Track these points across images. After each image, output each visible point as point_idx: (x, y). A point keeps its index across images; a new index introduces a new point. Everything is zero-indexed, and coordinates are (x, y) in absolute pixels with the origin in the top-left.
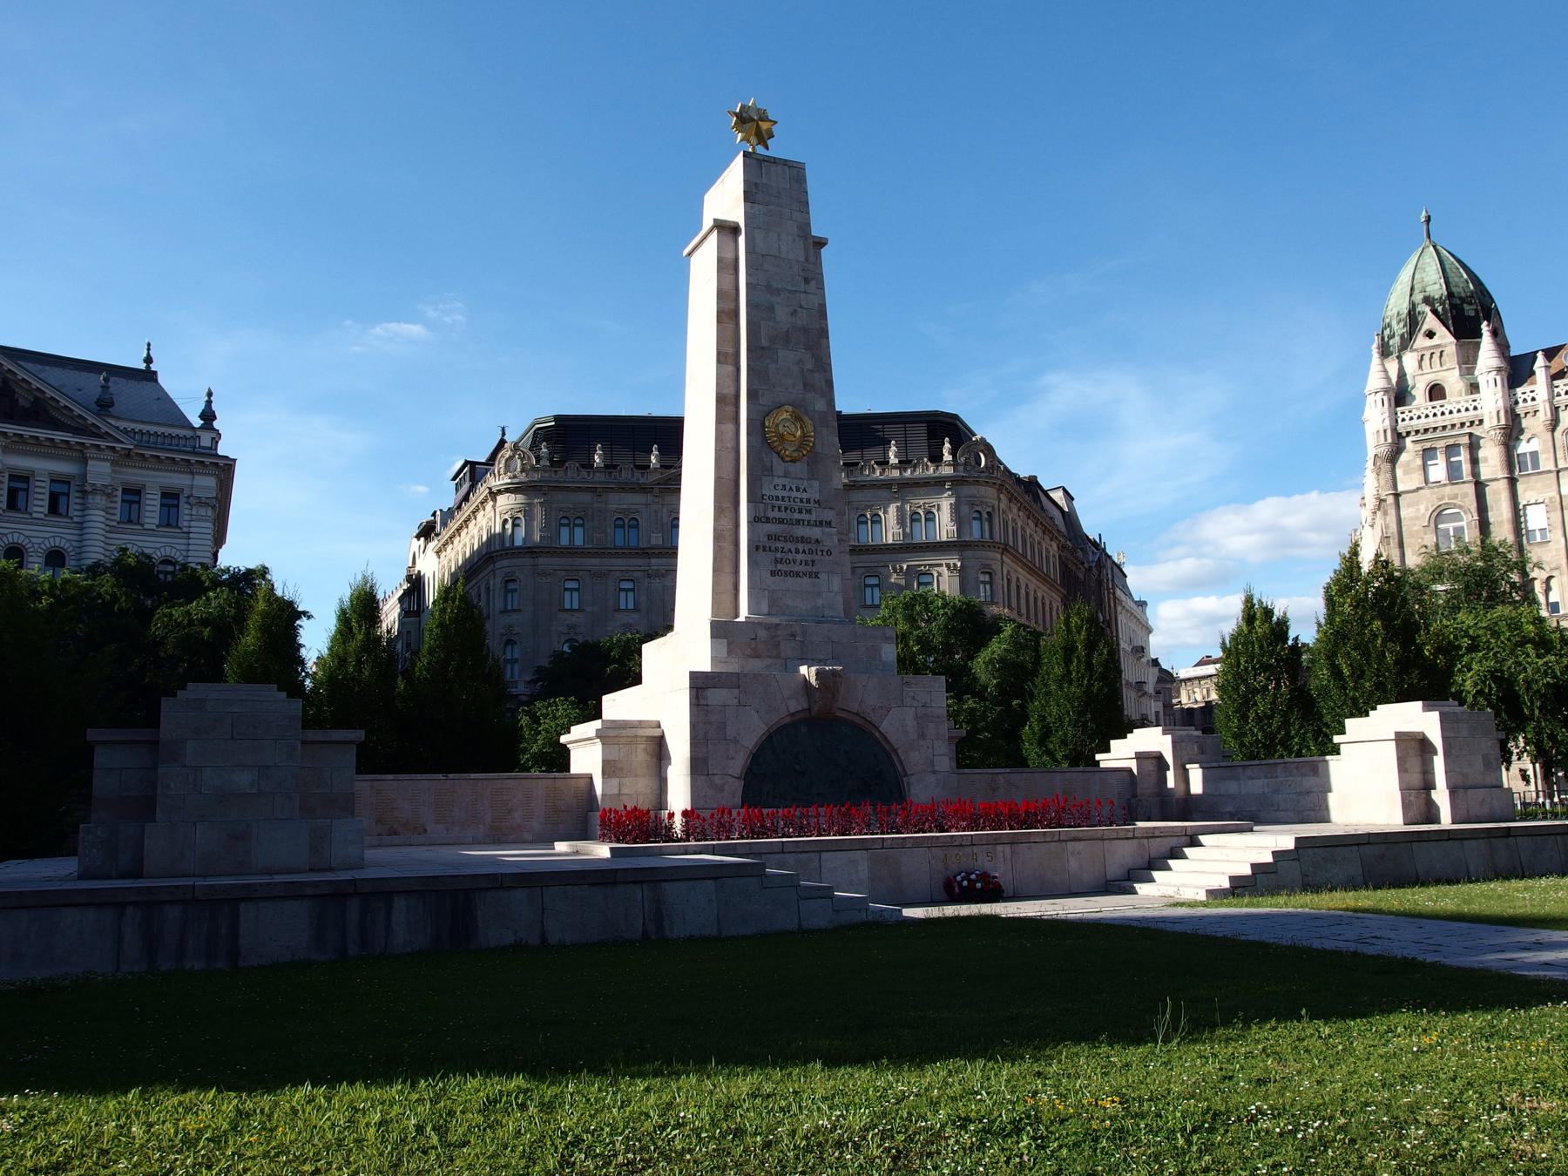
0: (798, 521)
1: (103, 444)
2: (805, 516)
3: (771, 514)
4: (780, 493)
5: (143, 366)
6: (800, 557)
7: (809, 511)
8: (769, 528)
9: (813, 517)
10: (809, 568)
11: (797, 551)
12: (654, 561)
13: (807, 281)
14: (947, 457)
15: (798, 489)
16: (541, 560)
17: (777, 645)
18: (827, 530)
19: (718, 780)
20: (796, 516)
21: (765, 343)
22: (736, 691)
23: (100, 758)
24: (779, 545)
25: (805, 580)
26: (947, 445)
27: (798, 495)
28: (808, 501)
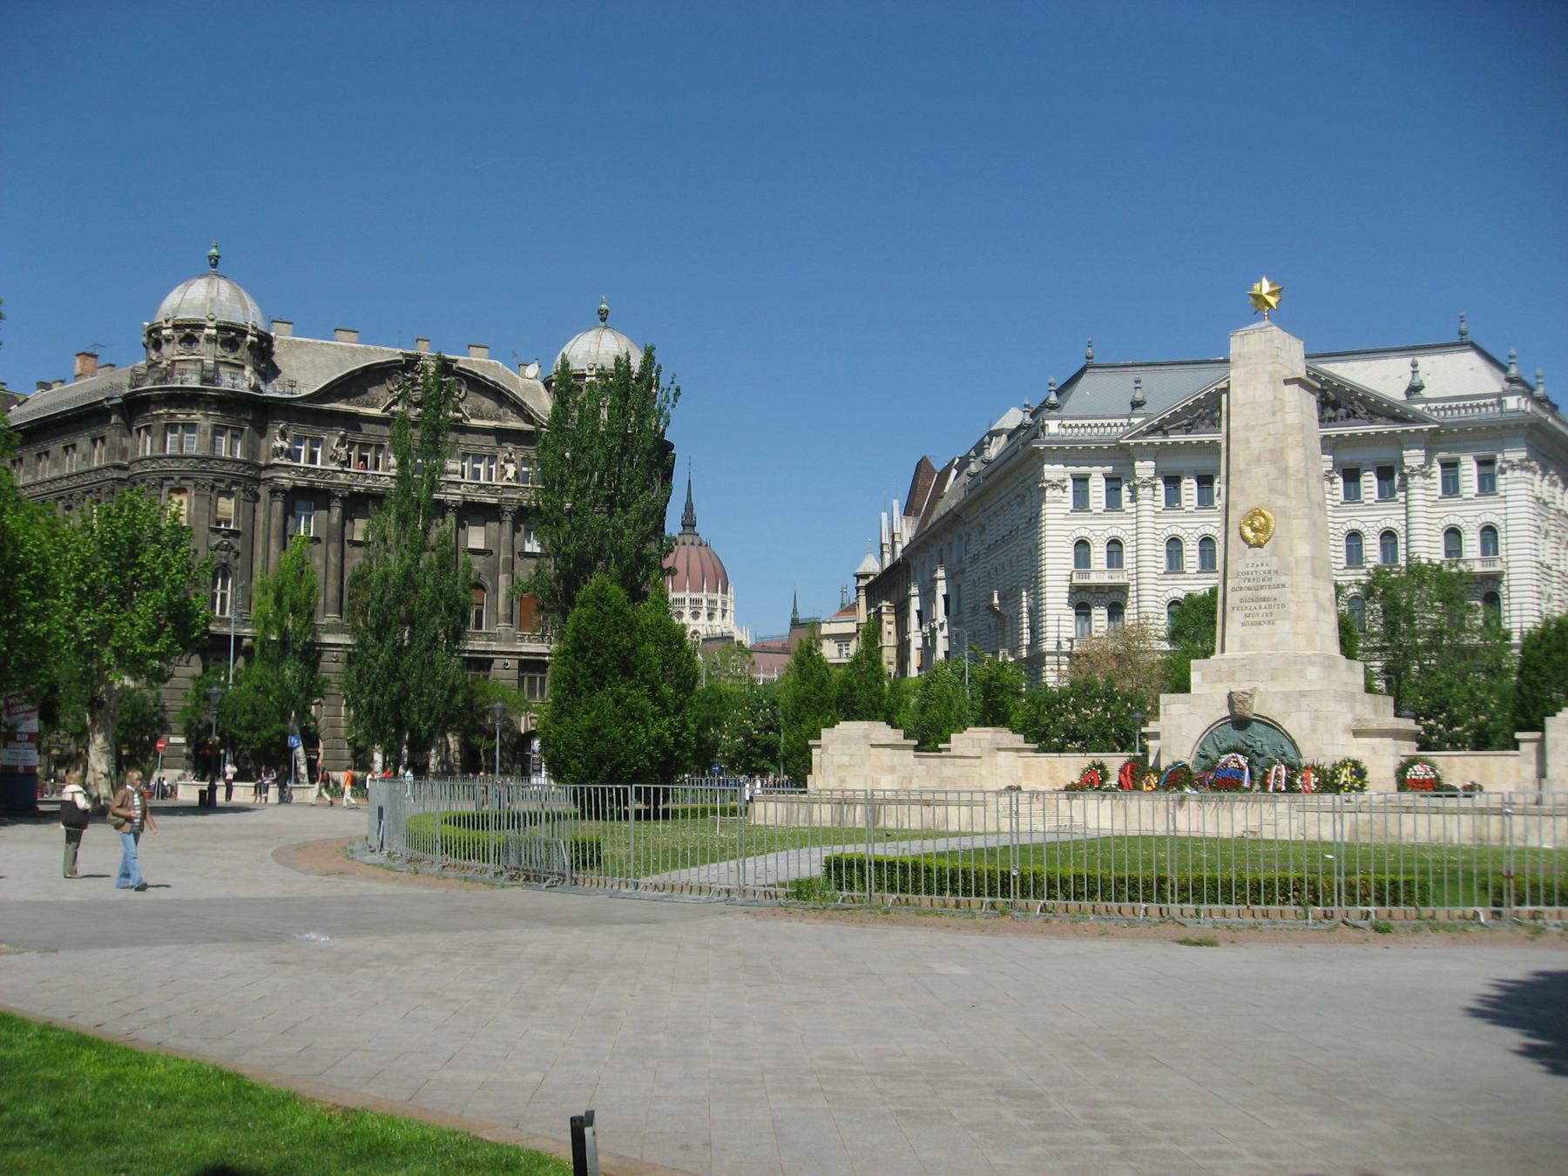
1: (1412, 428)
3: (1243, 585)
4: (1250, 569)
5: (1457, 339)
9: (1273, 582)
17: (1233, 673)
21: (1242, 466)
23: (814, 751)
25: (1265, 627)
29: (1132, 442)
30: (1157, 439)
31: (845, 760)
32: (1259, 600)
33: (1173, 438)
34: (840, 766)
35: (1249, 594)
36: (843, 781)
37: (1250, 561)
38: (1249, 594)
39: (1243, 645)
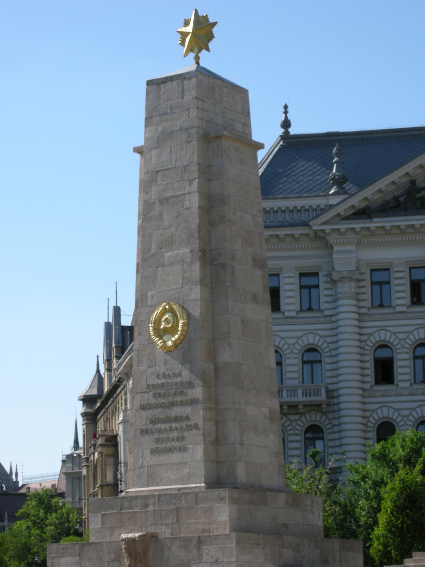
2: (178, 399)
6: (175, 434)
7: (182, 393)
8: (150, 412)
21: (153, 251)
24: (158, 426)
29: (327, 228)
30: (358, 225)
32: (168, 420)
33: (376, 223)
35: (158, 412)
38: (158, 412)
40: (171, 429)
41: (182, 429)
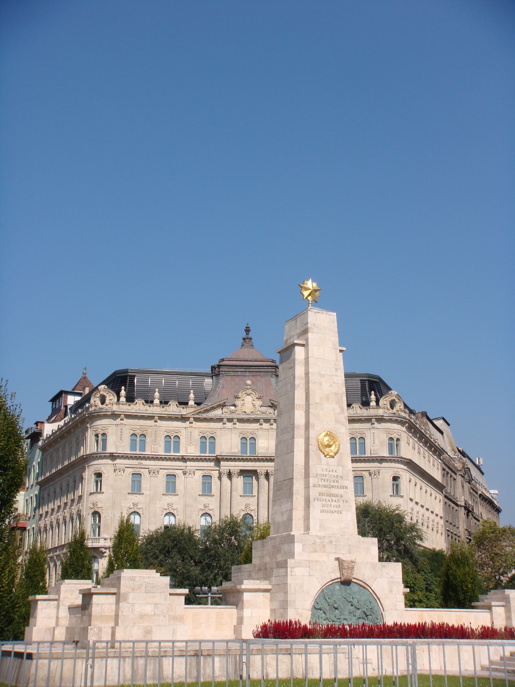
0: (333, 487)
2: (335, 484)
3: (321, 483)
4: (325, 473)
6: (333, 503)
7: (337, 482)
9: (339, 484)
10: (337, 509)
11: (332, 501)
12: (189, 463)
13: (336, 369)
14: (373, 404)
15: (332, 471)
16: (118, 461)
17: (324, 546)
18: (345, 490)
19: (300, 611)
20: (332, 484)
21: (318, 401)
22: (308, 569)
24: (324, 498)
25: (336, 514)
26: (373, 397)
27: (333, 474)
28: (337, 476)
31: (149, 609)
32: (330, 495)
34: (142, 617)
35: (324, 490)
36: (148, 632)
37: (325, 467)
38: (324, 490)
39: (322, 527)
40: (332, 501)
41: (339, 501)
